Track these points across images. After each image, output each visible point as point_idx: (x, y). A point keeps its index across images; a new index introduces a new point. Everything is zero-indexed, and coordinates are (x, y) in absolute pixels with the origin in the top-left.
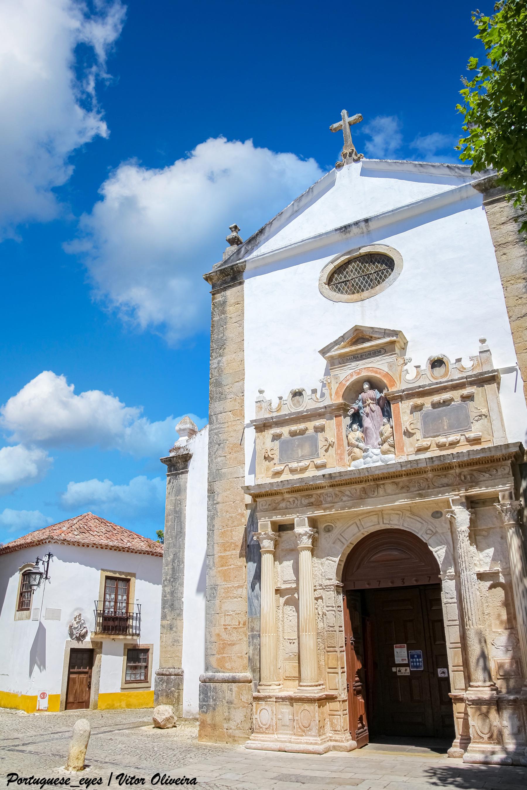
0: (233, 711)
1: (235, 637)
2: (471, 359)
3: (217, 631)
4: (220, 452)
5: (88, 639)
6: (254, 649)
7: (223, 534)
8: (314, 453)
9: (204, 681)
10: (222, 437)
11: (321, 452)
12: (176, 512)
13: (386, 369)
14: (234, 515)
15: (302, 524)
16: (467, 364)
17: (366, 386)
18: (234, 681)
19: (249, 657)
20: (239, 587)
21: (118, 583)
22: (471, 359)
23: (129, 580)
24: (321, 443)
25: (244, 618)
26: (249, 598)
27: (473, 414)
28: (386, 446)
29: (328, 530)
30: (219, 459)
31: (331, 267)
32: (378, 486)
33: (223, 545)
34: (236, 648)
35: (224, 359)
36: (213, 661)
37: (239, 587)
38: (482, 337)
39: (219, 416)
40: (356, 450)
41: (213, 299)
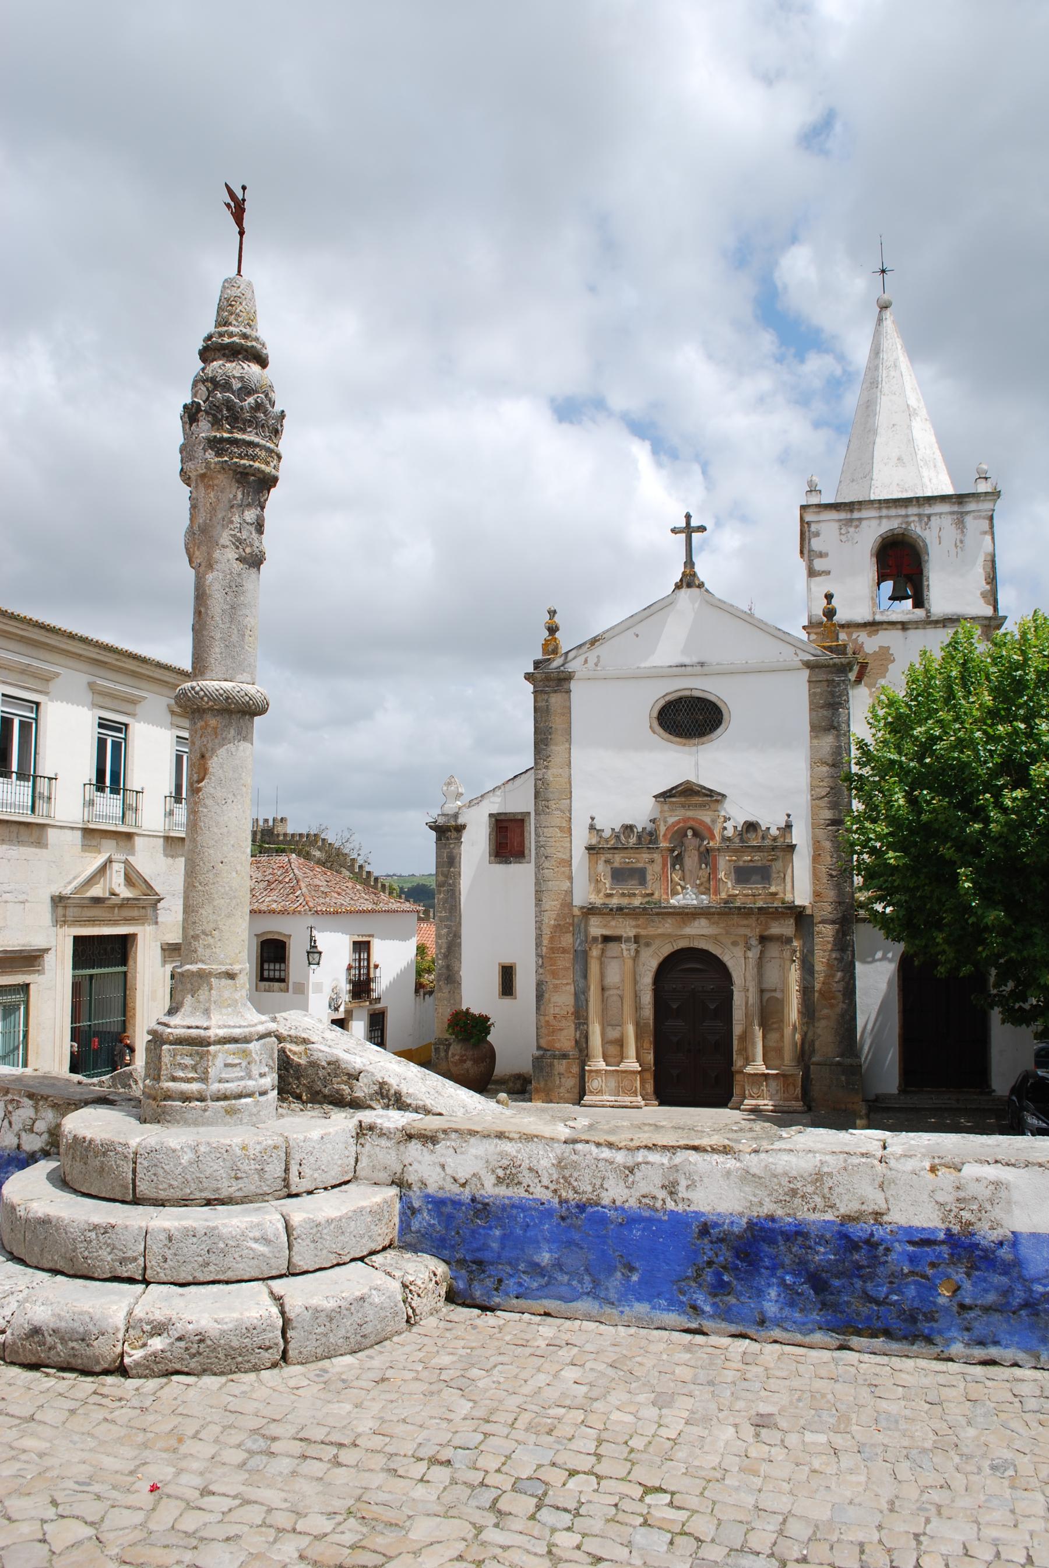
0: (563, 1080)
1: (563, 1023)
2: (778, 829)
3: (547, 1018)
4: (546, 864)
5: (342, 1009)
6: (581, 1034)
7: (552, 939)
8: (643, 882)
9: (537, 1058)
10: (549, 851)
11: (649, 883)
12: (450, 885)
13: (710, 824)
14: (562, 923)
15: (628, 940)
16: (774, 832)
17: (690, 833)
18: (565, 1056)
19: (576, 1041)
20: (567, 984)
21: (362, 947)
22: (778, 829)
23: (369, 942)
24: (649, 877)
25: (571, 1010)
26: (575, 994)
27: (774, 875)
28: (702, 889)
29: (648, 945)
30: (546, 871)
31: (662, 703)
32: (695, 919)
33: (552, 948)
34: (565, 1032)
35: (550, 772)
36: (543, 1043)
37: (567, 984)
38: (789, 812)
39: (546, 830)
40: (679, 887)
41: (535, 701)
